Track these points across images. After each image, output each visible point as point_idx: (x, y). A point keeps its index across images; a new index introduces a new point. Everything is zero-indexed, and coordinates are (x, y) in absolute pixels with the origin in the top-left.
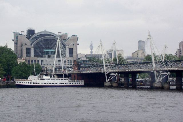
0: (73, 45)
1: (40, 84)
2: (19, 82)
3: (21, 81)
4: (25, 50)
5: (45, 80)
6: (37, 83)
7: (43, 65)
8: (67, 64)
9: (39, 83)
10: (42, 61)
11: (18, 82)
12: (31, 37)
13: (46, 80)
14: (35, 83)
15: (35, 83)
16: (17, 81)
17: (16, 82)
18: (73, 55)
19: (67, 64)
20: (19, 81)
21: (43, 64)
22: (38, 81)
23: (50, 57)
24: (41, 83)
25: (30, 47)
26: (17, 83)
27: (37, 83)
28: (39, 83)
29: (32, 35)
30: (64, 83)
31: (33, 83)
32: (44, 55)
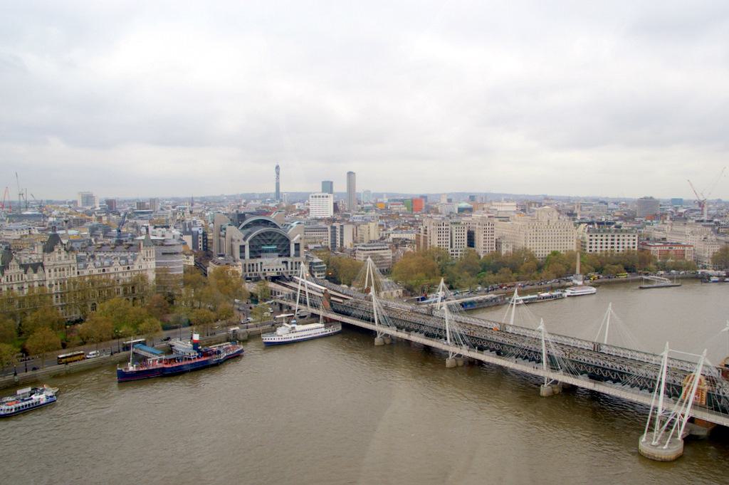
0: (301, 239)
1: (293, 339)
8: (294, 268)
10: (261, 263)
12: (240, 224)
19: (294, 268)
21: (263, 268)
24: (292, 337)
25: (242, 243)
26: (264, 341)
32: (262, 254)
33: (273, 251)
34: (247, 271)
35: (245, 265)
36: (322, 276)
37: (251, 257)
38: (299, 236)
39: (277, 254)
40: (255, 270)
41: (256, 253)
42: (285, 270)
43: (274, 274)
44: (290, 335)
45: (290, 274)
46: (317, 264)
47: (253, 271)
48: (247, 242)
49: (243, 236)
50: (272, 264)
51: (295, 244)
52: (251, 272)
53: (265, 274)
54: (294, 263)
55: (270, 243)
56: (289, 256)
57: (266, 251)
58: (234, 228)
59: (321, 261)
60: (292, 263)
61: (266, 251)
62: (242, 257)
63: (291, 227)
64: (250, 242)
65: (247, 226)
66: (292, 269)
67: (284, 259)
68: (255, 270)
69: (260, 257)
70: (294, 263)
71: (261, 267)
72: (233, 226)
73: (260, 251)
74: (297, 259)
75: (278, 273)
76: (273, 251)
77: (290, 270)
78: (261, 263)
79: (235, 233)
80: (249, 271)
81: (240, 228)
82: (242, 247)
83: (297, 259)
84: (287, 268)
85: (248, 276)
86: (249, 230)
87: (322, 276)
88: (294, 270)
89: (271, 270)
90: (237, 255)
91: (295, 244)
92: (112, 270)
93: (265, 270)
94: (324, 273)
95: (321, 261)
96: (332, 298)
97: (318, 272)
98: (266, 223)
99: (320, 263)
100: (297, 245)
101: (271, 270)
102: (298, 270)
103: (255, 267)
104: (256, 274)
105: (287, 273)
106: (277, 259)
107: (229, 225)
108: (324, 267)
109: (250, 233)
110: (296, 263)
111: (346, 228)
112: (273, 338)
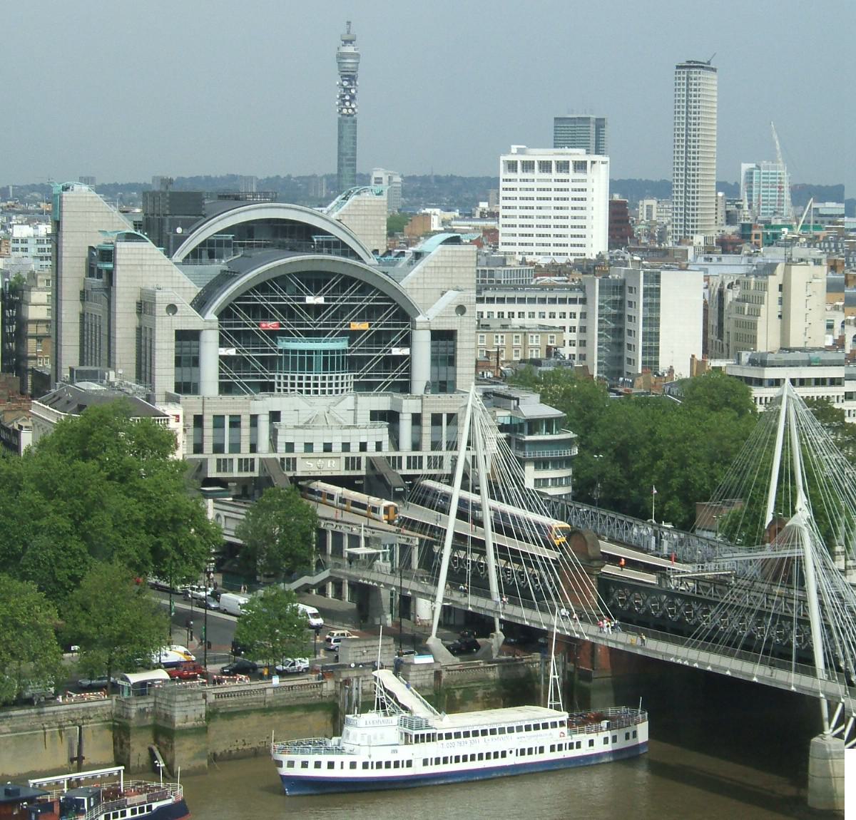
0: (461, 309)
1: (418, 769)
2: (298, 764)
3: (312, 759)
4: (165, 346)
5: (440, 737)
6: (397, 764)
7: (281, 453)
9: (409, 764)
10: (275, 416)
11: (291, 764)
13: (449, 736)
14: (388, 765)
15: (388, 765)
16: (285, 758)
17: (279, 764)
18: (459, 370)
19: (426, 442)
20: (299, 758)
21: (282, 440)
22: (405, 753)
23: (319, 389)
24: (419, 759)
25: (189, 319)
26: (285, 771)
27: (397, 764)
28: (409, 764)
29: (190, 226)
30: (541, 750)
31: (379, 765)
32: (277, 377)
33: (331, 362)
34: (208, 446)
35: (199, 420)
36: (557, 482)
37: (226, 388)
38: (452, 297)
39: (350, 377)
40: (245, 447)
41: (252, 370)
42: (387, 451)
43: (335, 467)
44: (405, 753)
45: (405, 471)
46: (533, 425)
47: (235, 448)
48: (211, 316)
49: (194, 290)
50: (321, 424)
51: (438, 336)
52: (227, 455)
53: (292, 463)
54: (427, 421)
55: (312, 323)
56: (405, 388)
58: (148, 249)
59: (549, 411)
60: (417, 419)
61: (305, 361)
62: (186, 387)
63: (418, 255)
64: (225, 314)
66: (416, 446)
67: (382, 402)
68: (245, 447)
69: (268, 388)
70: (427, 421)
71: (274, 433)
72: (149, 246)
73: (269, 363)
74: (443, 404)
75: (352, 463)
76: (331, 362)
77: (406, 450)
78: (275, 416)
79: (149, 270)
80: (218, 448)
81: (180, 255)
82: (188, 338)
83: (443, 404)
84: (396, 444)
85: (212, 472)
87: (557, 482)
88: (426, 452)
89: (318, 448)
90: (165, 375)
91: (438, 336)
93: (290, 447)
94: (567, 472)
95: (549, 411)
96: (609, 569)
97: (541, 464)
98: (301, 235)
99: (549, 424)
100: (444, 338)
101: (318, 448)
102: (447, 455)
103: (245, 431)
104: (246, 464)
105: (396, 462)
106: (349, 400)
107: (130, 237)
108: (568, 443)
109: (226, 277)
110: (436, 419)
111: (669, 281)
112: (325, 759)
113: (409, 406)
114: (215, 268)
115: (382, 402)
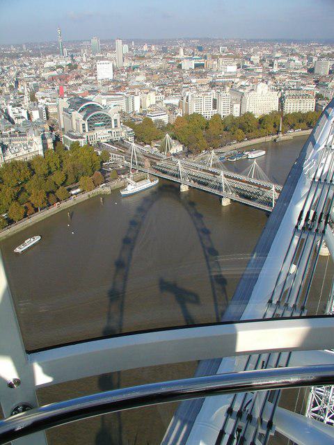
24: (137, 189)
33: (102, 125)
41: (92, 128)
43: (106, 141)
50: (102, 134)
57: (98, 126)
61: (98, 126)
65: (83, 109)
67: (110, 130)
73: (94, 126)
76: (102, 125)
86: (84, 113)
92: (20, 154)
113: (113, 131)
114: (84, 113)
115: (110, 130)
